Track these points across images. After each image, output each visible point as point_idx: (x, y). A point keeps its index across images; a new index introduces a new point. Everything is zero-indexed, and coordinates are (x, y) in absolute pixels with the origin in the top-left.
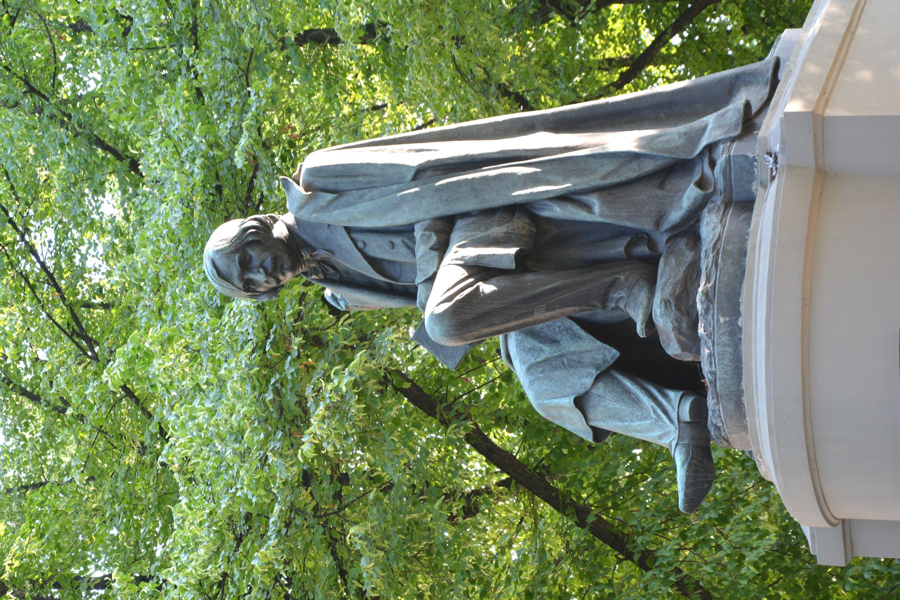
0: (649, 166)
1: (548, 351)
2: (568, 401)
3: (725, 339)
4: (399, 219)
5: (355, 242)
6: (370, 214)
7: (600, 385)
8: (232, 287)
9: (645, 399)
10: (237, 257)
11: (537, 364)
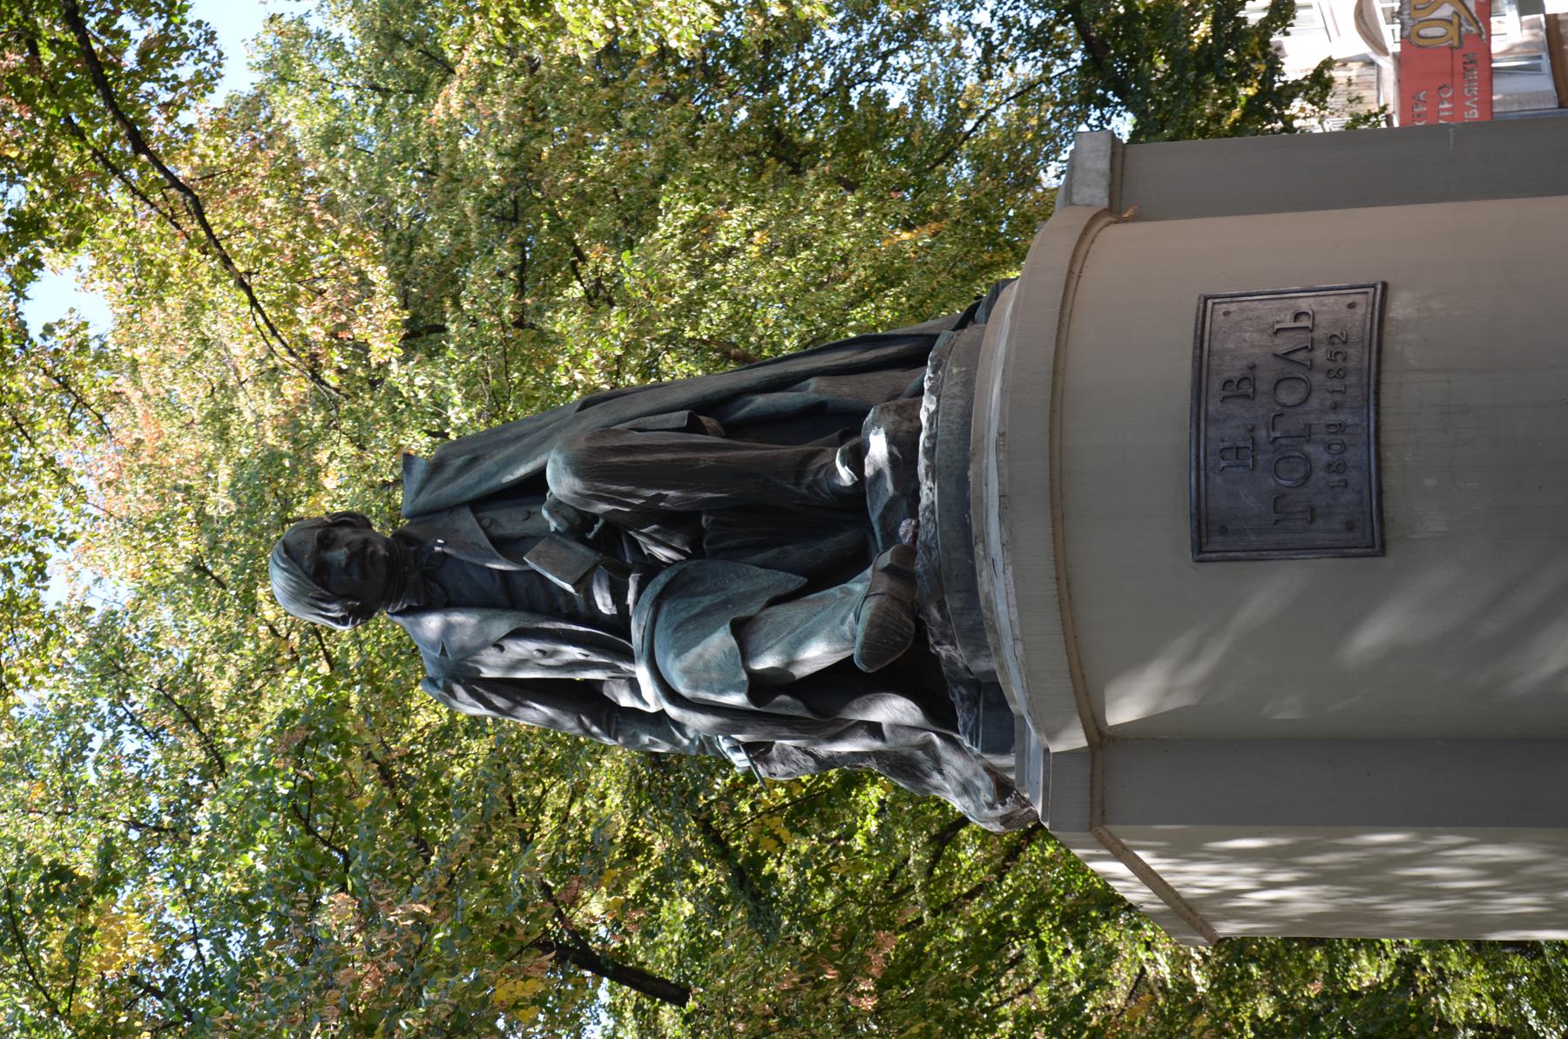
1: (707, 601)
3: (956, 390)
5: (479, 521)
7: (773, 609)
8: (299, 572)
9: (835, 591)
11: (689, 620)
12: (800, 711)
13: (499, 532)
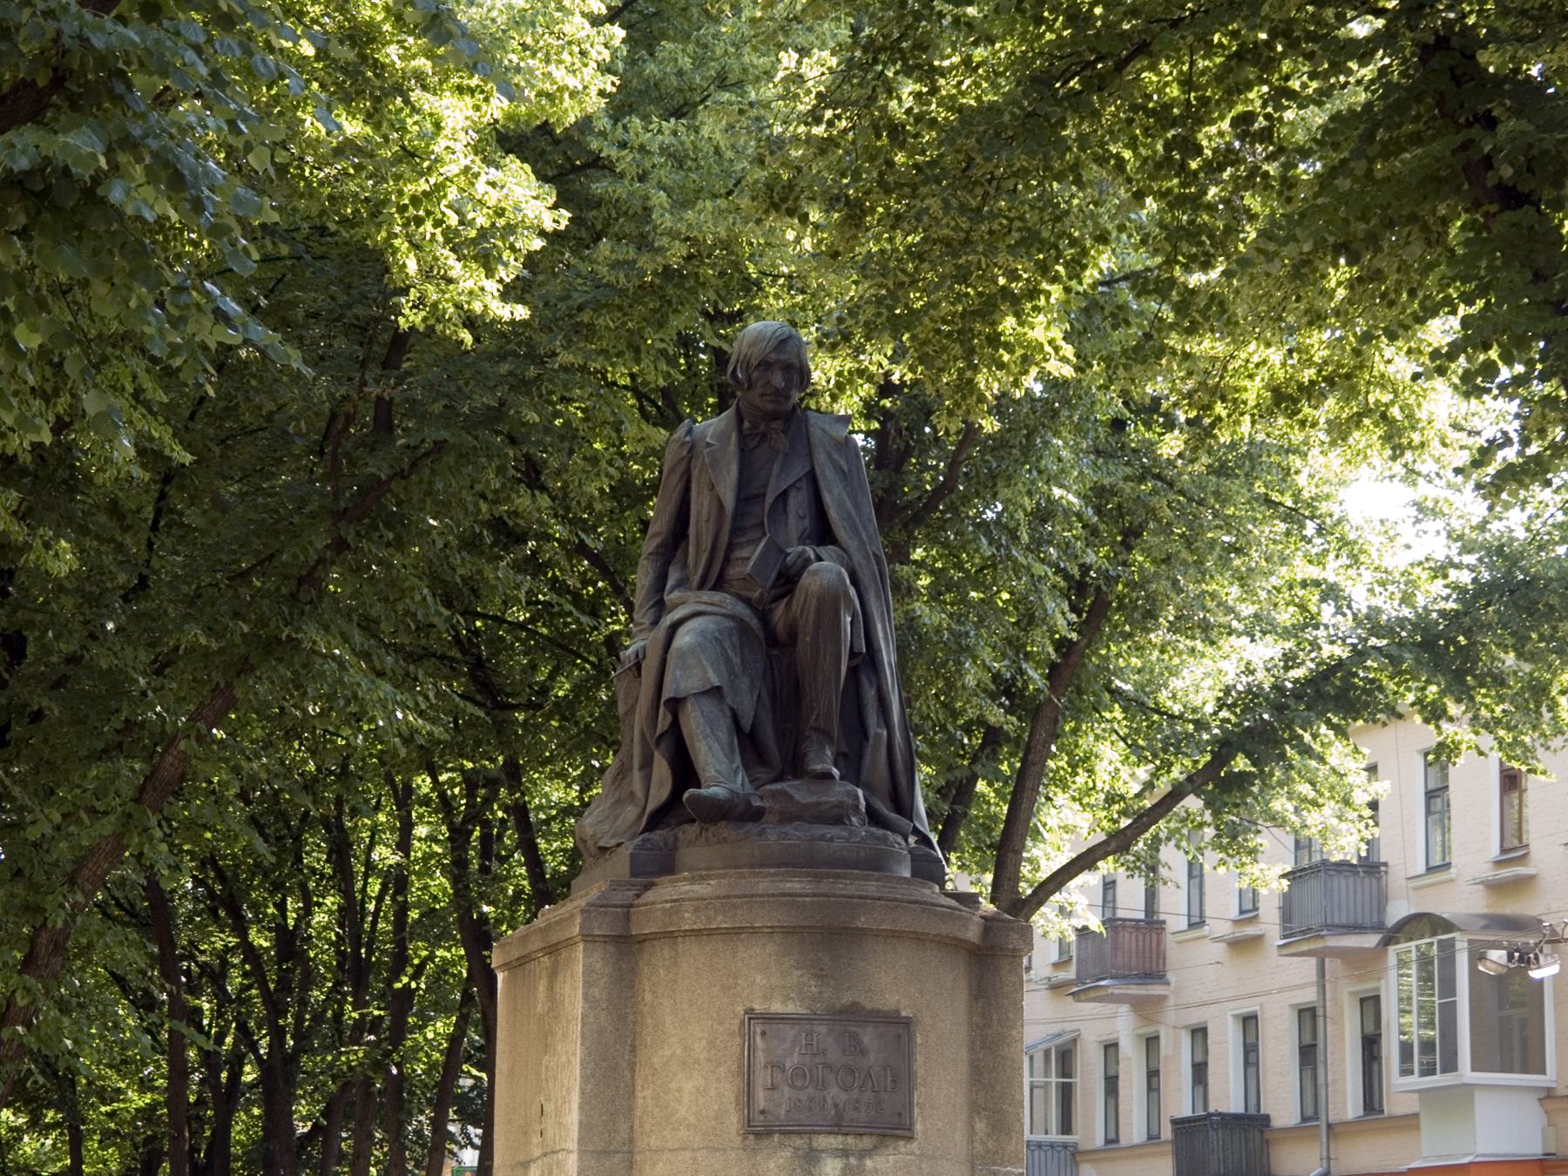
0: (903, 780)
1: (737, 660)
2: (715, 681)
4: (842, 533)
5: (800, 480)
6: (841, 505)
7: (729, 713)
9: (738, 759)
10: (796, 361)
12: (660, 728)
13: (792, 494)
